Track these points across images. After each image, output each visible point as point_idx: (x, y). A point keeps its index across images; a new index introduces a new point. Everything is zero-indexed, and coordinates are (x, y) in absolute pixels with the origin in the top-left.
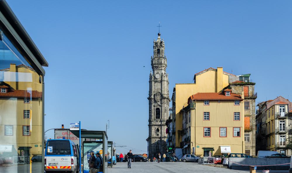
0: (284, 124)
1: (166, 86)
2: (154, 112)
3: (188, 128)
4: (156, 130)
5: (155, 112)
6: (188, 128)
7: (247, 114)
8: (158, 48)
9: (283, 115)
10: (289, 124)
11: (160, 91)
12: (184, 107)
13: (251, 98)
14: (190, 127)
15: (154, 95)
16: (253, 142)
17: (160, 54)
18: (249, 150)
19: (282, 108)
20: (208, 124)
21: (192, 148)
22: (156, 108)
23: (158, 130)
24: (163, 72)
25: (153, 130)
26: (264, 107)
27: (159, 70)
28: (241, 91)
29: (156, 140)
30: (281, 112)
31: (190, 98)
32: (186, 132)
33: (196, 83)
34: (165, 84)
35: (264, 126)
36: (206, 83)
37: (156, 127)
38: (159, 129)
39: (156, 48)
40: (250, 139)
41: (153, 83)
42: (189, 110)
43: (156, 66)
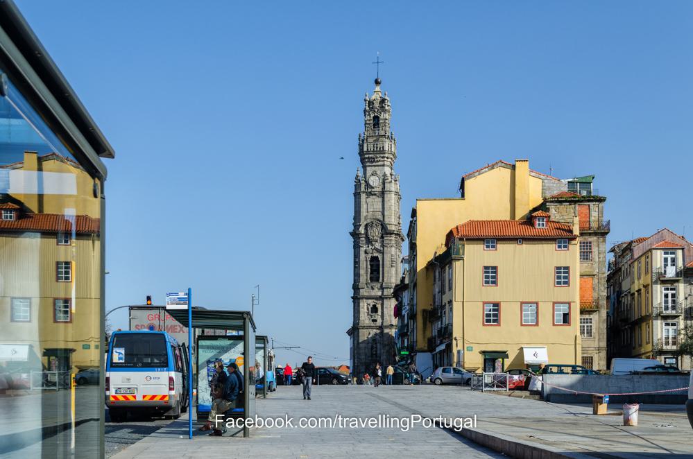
0: (673, 296)
1: (393, 204)
2: (365, 266)
3: (445, 305)
4: (370, 308)
5: (369, 267)
6: (447, 305)
7: (587, 270)
8: (376, 114)
9: (671, 272)
10: (687, 296)
11: (380, 217)
12: (437, 255)
13: (595, 234)
14: (450, 302)
15: (366, 226)
16: (601, 337)
17: (381, 128)
18: (592, 357)
19: (669, 257)
20: (493, 294)
21: (455, 351)
22: (370, 256)
23: (375, 309)
24: (387, 170)
25: (363, 308)
26: (627, 255)
27: (378, 166)
28: (572, 217)
29: (369, 334)
30: (666, 265)
31: (451, 232)
32: (441, 313)
33: (465, 197)
34: (391, 199)
35: (626, 300)
36: (488, 197)
37: (371, 302)
38: (377, 306)
39: (369, 115)
40: (593, 331)
41: (363, 196)
42: (447, 261)
43: (370, 156)
